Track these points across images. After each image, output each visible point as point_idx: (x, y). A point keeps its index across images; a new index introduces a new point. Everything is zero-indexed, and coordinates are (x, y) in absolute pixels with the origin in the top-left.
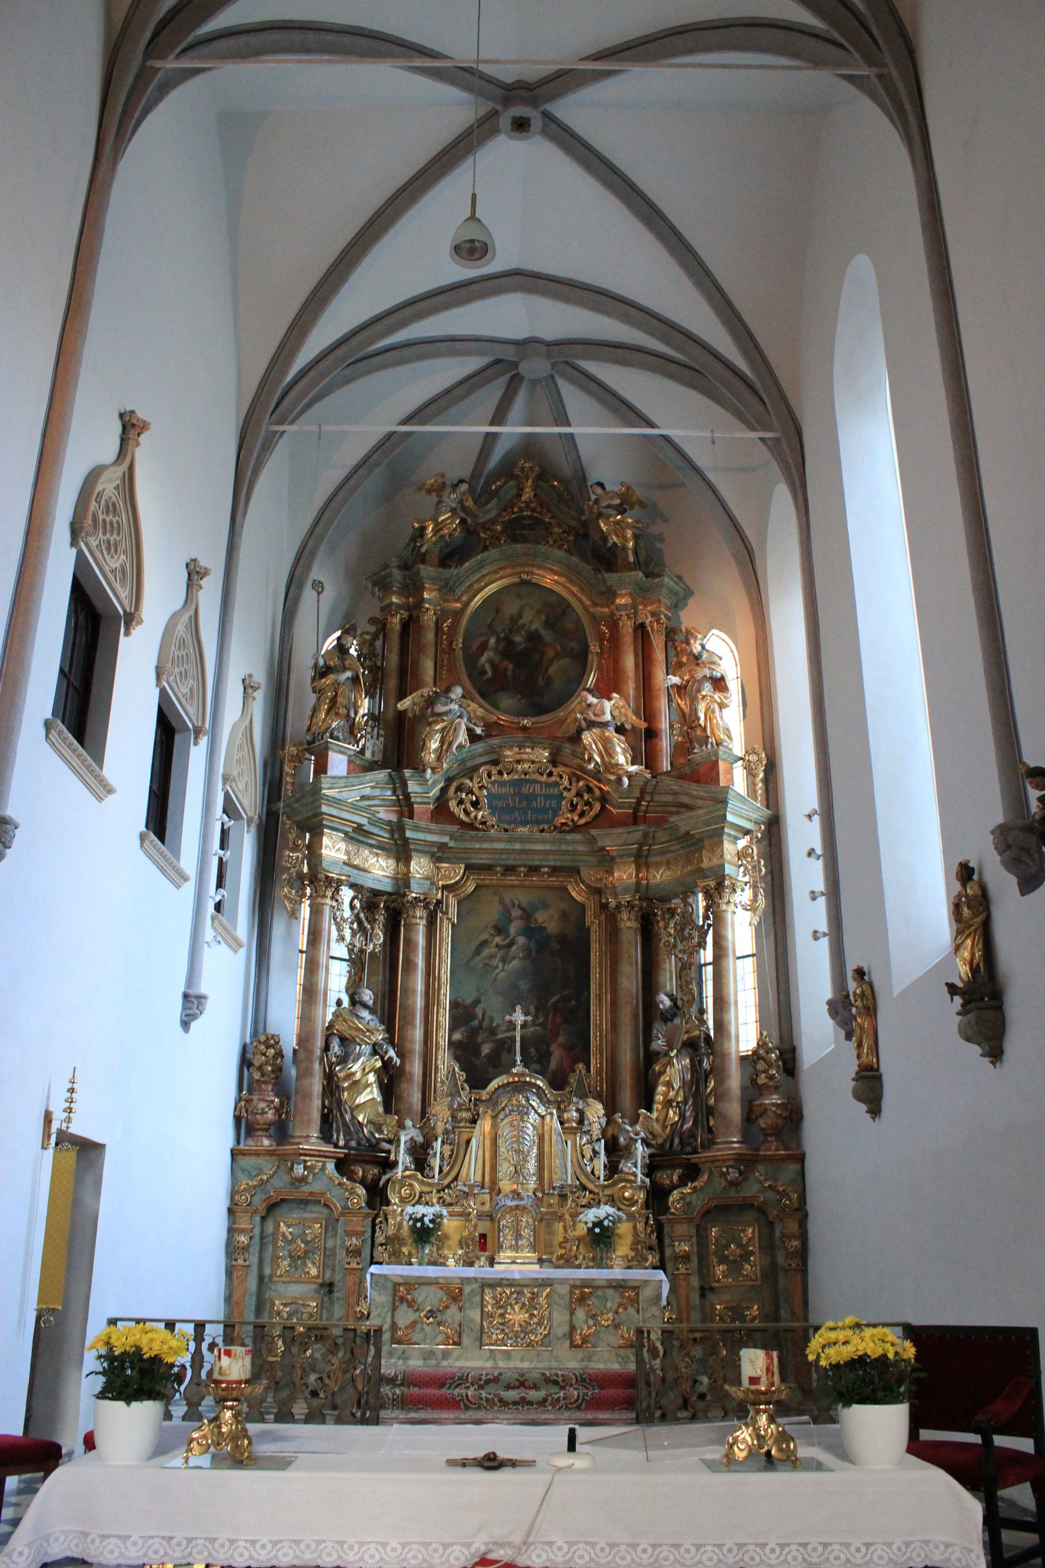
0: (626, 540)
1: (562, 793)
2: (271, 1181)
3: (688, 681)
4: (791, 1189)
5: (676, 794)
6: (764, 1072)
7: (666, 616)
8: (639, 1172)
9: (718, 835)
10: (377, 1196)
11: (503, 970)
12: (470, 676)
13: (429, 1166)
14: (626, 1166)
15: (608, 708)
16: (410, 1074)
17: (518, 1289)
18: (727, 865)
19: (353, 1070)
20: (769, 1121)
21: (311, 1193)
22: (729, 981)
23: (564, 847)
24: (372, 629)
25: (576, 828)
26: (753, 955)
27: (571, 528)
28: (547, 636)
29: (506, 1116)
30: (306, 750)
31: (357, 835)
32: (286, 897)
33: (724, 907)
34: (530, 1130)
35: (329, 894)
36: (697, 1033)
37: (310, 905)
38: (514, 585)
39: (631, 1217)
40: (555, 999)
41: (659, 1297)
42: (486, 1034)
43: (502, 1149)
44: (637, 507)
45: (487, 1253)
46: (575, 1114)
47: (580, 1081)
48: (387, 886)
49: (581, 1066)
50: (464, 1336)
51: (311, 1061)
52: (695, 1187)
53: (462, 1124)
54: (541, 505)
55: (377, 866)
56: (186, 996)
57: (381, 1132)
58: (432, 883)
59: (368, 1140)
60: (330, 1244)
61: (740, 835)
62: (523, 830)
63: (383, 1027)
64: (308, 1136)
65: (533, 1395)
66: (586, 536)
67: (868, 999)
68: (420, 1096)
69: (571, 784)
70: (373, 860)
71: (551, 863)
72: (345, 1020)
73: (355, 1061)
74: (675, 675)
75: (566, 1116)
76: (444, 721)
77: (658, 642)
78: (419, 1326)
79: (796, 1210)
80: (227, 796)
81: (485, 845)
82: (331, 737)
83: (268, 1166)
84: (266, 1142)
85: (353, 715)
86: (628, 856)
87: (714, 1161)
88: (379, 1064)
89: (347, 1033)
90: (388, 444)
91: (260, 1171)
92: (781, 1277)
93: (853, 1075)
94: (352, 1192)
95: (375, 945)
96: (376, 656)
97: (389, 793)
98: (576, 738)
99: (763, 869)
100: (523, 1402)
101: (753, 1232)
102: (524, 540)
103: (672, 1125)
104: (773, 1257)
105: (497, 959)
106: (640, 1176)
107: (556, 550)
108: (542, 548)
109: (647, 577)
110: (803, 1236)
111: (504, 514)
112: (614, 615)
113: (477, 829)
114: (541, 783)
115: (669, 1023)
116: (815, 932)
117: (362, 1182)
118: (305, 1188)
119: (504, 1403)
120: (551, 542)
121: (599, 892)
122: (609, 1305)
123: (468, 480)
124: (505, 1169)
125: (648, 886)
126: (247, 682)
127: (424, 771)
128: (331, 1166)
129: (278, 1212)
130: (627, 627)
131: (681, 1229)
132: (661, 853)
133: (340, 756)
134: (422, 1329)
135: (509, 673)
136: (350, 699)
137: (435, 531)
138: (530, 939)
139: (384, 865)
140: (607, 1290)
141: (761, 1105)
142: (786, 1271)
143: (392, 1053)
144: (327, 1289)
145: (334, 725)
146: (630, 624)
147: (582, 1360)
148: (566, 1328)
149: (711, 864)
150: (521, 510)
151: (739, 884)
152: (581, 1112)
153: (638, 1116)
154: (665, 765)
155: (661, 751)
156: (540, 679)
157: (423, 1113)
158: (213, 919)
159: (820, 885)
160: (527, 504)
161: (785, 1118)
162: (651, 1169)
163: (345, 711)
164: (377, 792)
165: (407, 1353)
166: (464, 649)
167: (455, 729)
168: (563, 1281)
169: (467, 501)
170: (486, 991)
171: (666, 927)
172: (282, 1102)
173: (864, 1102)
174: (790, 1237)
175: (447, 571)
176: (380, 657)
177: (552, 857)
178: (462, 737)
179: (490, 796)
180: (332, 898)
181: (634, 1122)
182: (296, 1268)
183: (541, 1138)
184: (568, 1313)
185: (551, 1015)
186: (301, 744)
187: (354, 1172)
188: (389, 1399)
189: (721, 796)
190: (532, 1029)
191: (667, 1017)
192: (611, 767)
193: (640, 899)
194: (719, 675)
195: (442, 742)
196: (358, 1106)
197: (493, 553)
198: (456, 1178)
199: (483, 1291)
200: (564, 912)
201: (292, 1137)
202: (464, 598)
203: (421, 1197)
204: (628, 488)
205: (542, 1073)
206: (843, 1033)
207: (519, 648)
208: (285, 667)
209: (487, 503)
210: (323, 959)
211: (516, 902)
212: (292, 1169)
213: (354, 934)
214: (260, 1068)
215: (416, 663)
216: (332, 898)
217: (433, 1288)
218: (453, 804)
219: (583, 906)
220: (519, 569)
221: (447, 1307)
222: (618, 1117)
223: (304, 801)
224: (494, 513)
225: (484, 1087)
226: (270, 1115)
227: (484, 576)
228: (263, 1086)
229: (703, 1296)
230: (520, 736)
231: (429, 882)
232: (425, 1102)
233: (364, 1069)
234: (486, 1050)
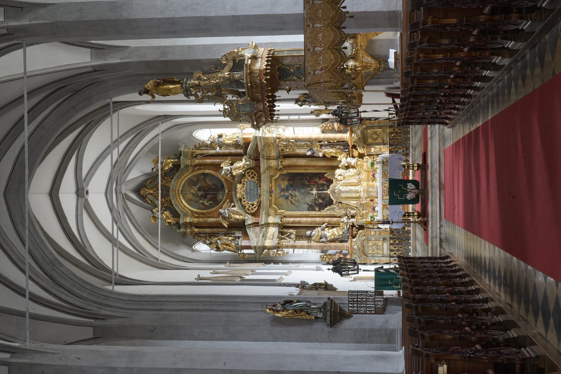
0: (171, 162)
3: (218, 145)
9: (264, 138)
10: (361, 227)
12: (212, 208)
14: (353, 164)
15: (226, 167)
16: (328, 221)
18: (273, 136)
25: (259, 176)
28: (199, 185)
31: (264, 236)
33: (284, 137)
37: (285, 248)
38: (182, 196)
45: (375, 199)
49: (325, 175)
54: (156, 187)
56: (317, 270)
59: (347, 231)
60: (373, 239)
61: (264, 132)
75: (340, 180)
81: (265, 202)
87: (351, 141)
88: (327, 229)
89: (319, 237)
90: (143, 233)
105: (296, 198)
122: (387, 168)
124: (354, 195)
125: (276, 157)
127: (245, 220)
128: (354, 240)
135: (211, 196)
137: (169, 219)
138: (290, 189)
143: (324, 225)
145: (234, 244)
149: (272, 140)
151: (278, 133)
155: (235, 152)
157: (340, 217)
162: (353, 157)
166: (204, 210)
171: (286, 151)
178: (235, 209)
179: (250, 201)
181: (340, 161)
183: (346, 185)
187: (355, 234)
189: (255, 138)
194: (217, 136)
195: (237, 214)
197: (173, 202)
200: (281, 180)
202: (187, 210)
208: (212, 261)
211: (279, 193)
214: (329, 259)
215: (209, 223)
218: (253, 212)
220: (177, 194)
222: (340, 166)
223: (257, 251)
227: (179, 204)
232: (336, 217)
234: (321, 201)
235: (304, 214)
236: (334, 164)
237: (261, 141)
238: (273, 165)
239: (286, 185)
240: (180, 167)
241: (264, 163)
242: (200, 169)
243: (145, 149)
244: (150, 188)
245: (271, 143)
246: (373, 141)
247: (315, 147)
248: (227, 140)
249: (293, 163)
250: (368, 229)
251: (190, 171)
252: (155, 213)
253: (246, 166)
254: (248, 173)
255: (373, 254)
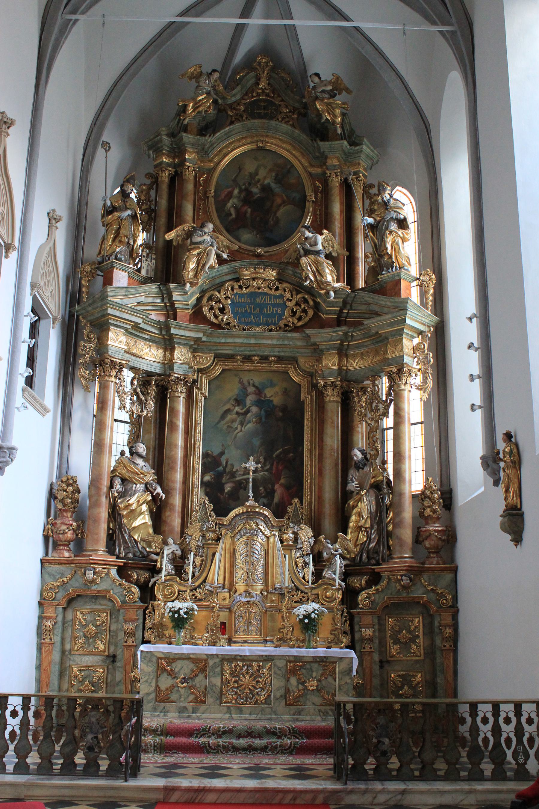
0: (335, 116)
1: (285, 303)
2: (70, 582)
3: (379, 222)
4: (447, 591)
5: (369, 304)
6: (429, 507)
7: (364, 176)
8: (337, 578)
11: (241, 431)
12: (219, 217)
13: (185, 572)
14: (327, 573)
17: (248, 663)
18: (405, 357)
19: (130, 502)
20: (432, 543)
21: (99, 591)
22: (405, 440)
23: (286, 342)
24: (148, 182)
25: (296, 329)
26: (422, 423)
27: (295, 109)
29: (241, 536)
30: (97, 268)
32: (81, 375)
33: (402, 387)
34: (258, 547)
35: (114, 374)
36: (381, 478)
38: (252, 150)
39: (330, 610)
40: (278, 452)
41: (351, 670)
42: (228, 477)
43: (238, 561)
44: (344, 92)
45: (226, 636)
46: (291, 535)
47: (296, 510)
48: (156, 368)
50: (208, 696)
51: (99, 495)
52: (378, 589)
53: (210, 542)
54: (274, 93)
55: (150, 353)
57: (150, 547)
58: (190, 367)
60: (114, 627)
61: (415, 335)
62: (257, 329)
63: (153, 471)
64: (97, 550)
65: (257, 742)
66: (305, 115)
67: (514, 455)
68: (180, 521)
69: (292, 296)
70: (146, 350)
71: (277, 354)
72: (125, 467)
73: (132, 495)
74: (369, 217)
76: (199, 248)
77: (358, 192)
78: (176, 689)
79: (450, 607)
80: (35, 299)
81: (230, 340)
82: (116, 259)
83: (67, 570)
84: (66, 554)
85: (132, 243)
86: (333, 349)
88: (150, 498)
89: (127, 475)
91: (62, 575)
92: (438, 654)
93: (502, 513)
94: (129, 590)
95: (148, 411)
96: (151, 202)
97: (159, 301)
98: (297, 264)
99: (432, 360)
100: (250, 749)
101: (419, 621)
102: (260, 117)
103: (362, 544)
104: (433, 641)
106: (338, 581)
107: (284, 125)
108: (273, 123)
109: (350, 145)
110: (455, 627)
111: (246, 97)
112: (326, 173)
113: (223, 328)
114: (270, 295)
115: (361, 470)
116: (473, 405)
117: (137, 583)
118: (94, 588)
119: (236, 749)
120: (280, 119)
121: (311, 375)
122: (314, 674)
123: (219, 70)
124: (240, 575)
126: (51, 215)
127: (185, 284)
128: (114, 572)
129: (75, 604)
130: (336, 182)
131: (368, 619)
132: (358, 346)
133: (122, 273)
134: (178, 691)
135: (248, 215)
136: (130, 231)
137: (195, 108)
138: (261, 409)
139: (155, 353)
140: (313, 664)
141: (426, 531)
142: (442, 650)
143: (159, 490)
144: (112, 659)
145: (118, 249)
146: (338, 179)
147: (294, 715)
148: (282, 691)
150: (258, 95)
151: (414, 370)
152: (296, 534)
153: (337, 537)
154: (361, 283)
155: (358, 273)
156: (271, 220)
158: (24, 390)
159: (476, 370)
160: (263, 90)
161: (444, 541)
162: (346, 575)
163: (127, 240)
164: (150, 300)
165: (167, 709)
166: (216, 196)
167: (208, 255)
168: (282, 657)
169: (218, 86)
170: (229, 446)
171: (359, 401)
172: (78, 526)
173: (510, 534)
174: (446, 626)
175: (203, 138)
176: (154, 202)
177: (277, 349)
178: (213, 260)
179: (233, 304)
180: (116, 377)
182: (89, 645)
183: (267, 553)
184: (284, 681)
185: (275, 463)
186: (94, 263)
187: (131, 576)
188: (151, 746)
189: (401, 305)
190: (261, 474)
191: (359, 466)
192: (323, 284)
193: (341, 381)
194: (402, 217)
195: (198, 263)
196: (134, 528)
197: (237, 126)
198: (204, 581)
199: (222, 665)
200: (286, 389)
201: (86, 551)
202: (216, 160)
203: (179, 594)
204: (338, 78)
205: (268, 506)
206: (491, 480)
207: (256, 197)
209: (233, 89)
210: (109, 421)
211: (251, 382)
212: (85, 574)
213: (133, 403)
214: (62, 501)
215: (180, 207)
216: (116, 377)
217: (186, 662)
218: (205, 310)
219: (300, 385)
220: (256, 138)
221: (196, 676)
222: (322, 537)
224: (238, 97)
225: (226, 516)
226: (70, 535)
227: (231, 143)
228: (65, 514)
229: (381, 667)
230: (255, 261)
231: (187, 366)
232: (184, 525)
233: (138, 501)
234: (228, 488)
235: (195, 443)
236: (328, 524)
237: (391, 325)
238: (324, 362)
239: (272, 401)
240: (322, 140)
241: (330, 341)
242: (316, 191)
243: (369, 47)
244: (272, 81)
245: (386, 352)
246: (389, 632)
247: (374, 470)
248: (393, 242)
249: (329, 414)
250: (141, 612)
251: (311, 170)
252: (209, 78)
253: (322, 292)
254: (306, 301)
255: (73, 626)
